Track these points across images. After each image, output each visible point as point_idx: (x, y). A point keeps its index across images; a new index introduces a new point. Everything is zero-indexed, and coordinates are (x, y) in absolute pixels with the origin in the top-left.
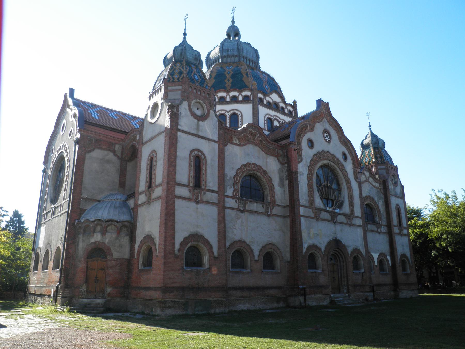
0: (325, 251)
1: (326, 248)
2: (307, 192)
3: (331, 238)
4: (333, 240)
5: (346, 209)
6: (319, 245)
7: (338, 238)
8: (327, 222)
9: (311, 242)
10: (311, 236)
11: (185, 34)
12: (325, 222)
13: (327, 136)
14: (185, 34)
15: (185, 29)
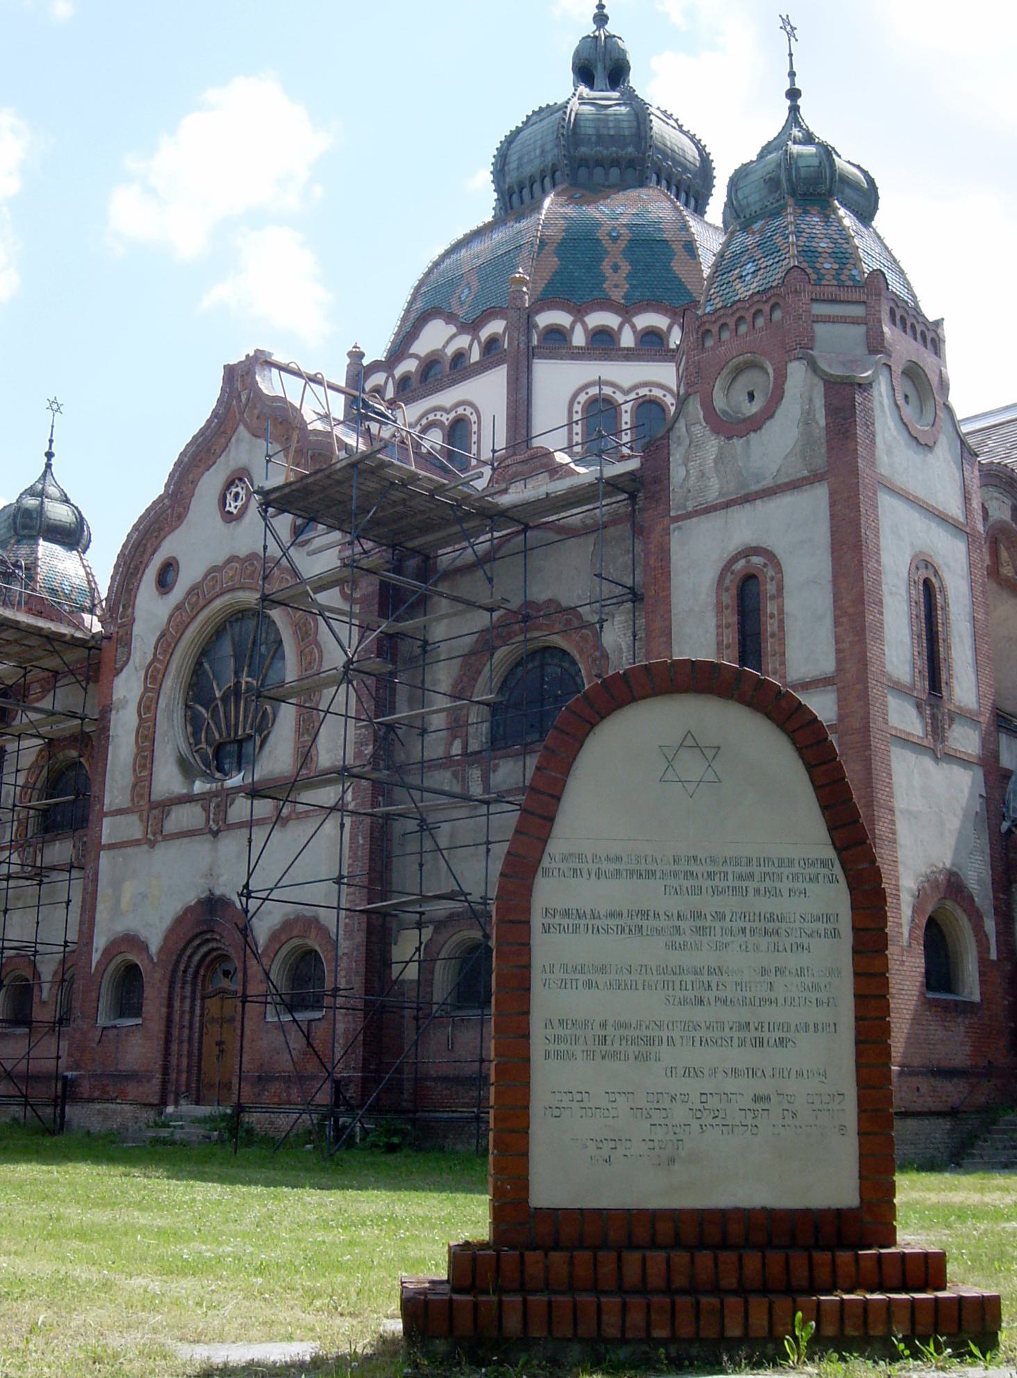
0: (161, 950)
1: (166, 938)
2: (130, 760)
3: (191, 898)
4: (200, 902)
5: (277, 757)
6: (144, 934)
7: (218, 892)
8: (186, 840)
9: (120, 927)
10: (124, 905)
11: (49, 455)
12: (177, 842)
13: (237, 495)
14: (49, 455)
15: (51, 441)
